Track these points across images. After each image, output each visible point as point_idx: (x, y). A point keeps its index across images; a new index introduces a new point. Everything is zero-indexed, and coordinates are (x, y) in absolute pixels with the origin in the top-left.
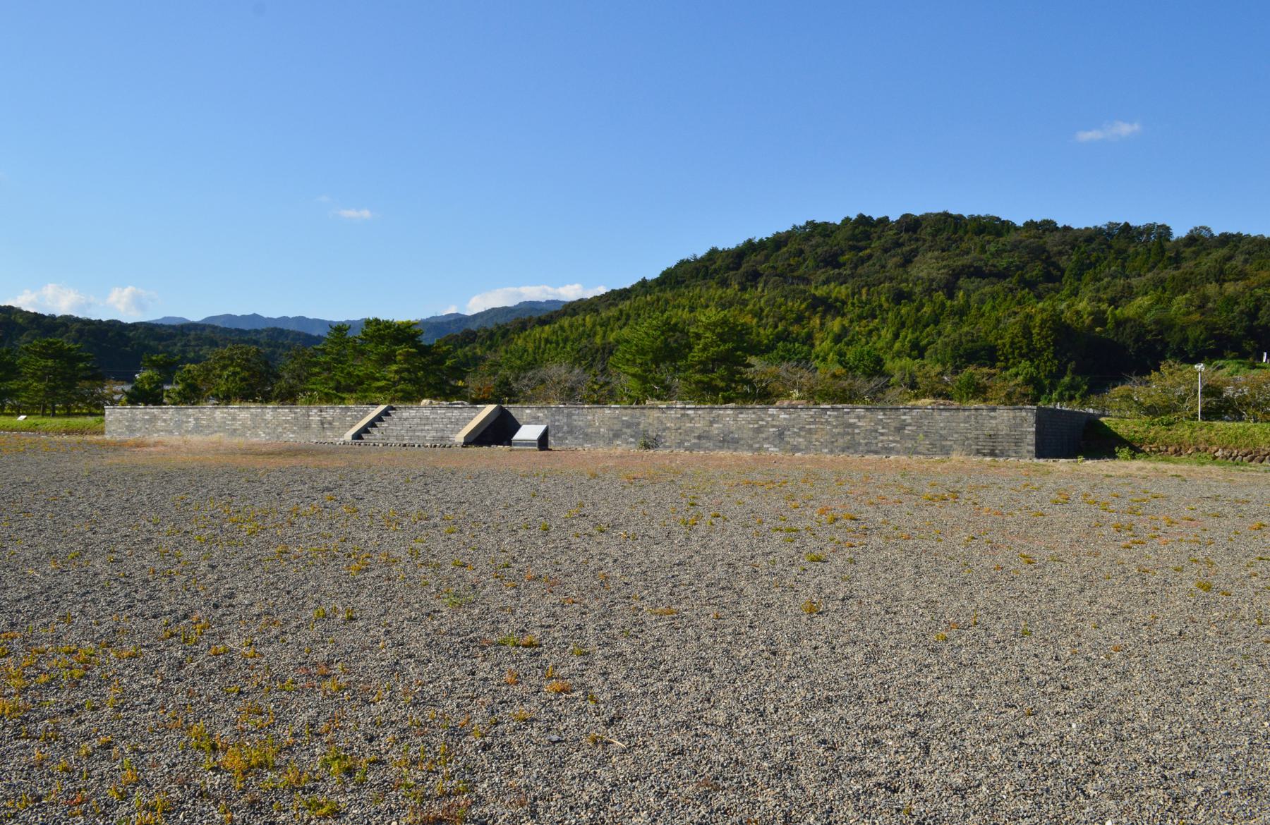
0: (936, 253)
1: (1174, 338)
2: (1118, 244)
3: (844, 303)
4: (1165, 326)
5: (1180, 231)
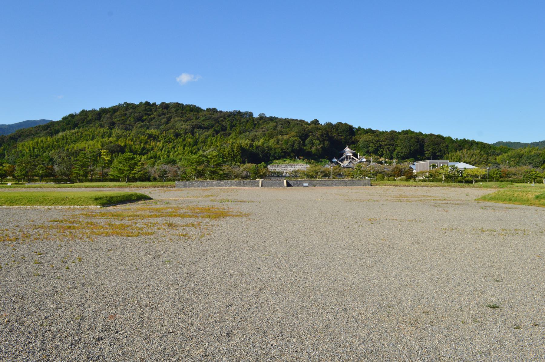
1: (272, 152)
2: (239, 117)
3: (158, 137)
4: (269, 148)
5: (256, 115)
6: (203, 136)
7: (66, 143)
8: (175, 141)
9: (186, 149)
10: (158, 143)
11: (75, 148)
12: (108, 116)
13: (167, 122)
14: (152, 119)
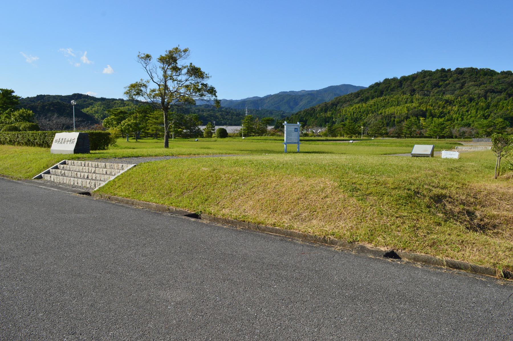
0: (473, 83)
3: (454, 102)
6: (495, 100)
7: (377, 108)
8: (469, 105)
9: (479, 112)
10: (454, 107)
11: (387, 113)
12: (408, 83)
13: (461, 88)
14: (447, 85)
